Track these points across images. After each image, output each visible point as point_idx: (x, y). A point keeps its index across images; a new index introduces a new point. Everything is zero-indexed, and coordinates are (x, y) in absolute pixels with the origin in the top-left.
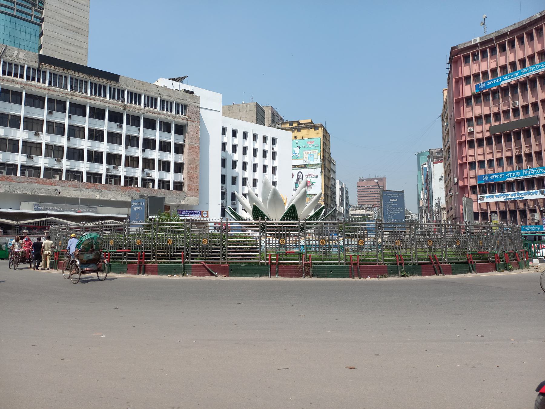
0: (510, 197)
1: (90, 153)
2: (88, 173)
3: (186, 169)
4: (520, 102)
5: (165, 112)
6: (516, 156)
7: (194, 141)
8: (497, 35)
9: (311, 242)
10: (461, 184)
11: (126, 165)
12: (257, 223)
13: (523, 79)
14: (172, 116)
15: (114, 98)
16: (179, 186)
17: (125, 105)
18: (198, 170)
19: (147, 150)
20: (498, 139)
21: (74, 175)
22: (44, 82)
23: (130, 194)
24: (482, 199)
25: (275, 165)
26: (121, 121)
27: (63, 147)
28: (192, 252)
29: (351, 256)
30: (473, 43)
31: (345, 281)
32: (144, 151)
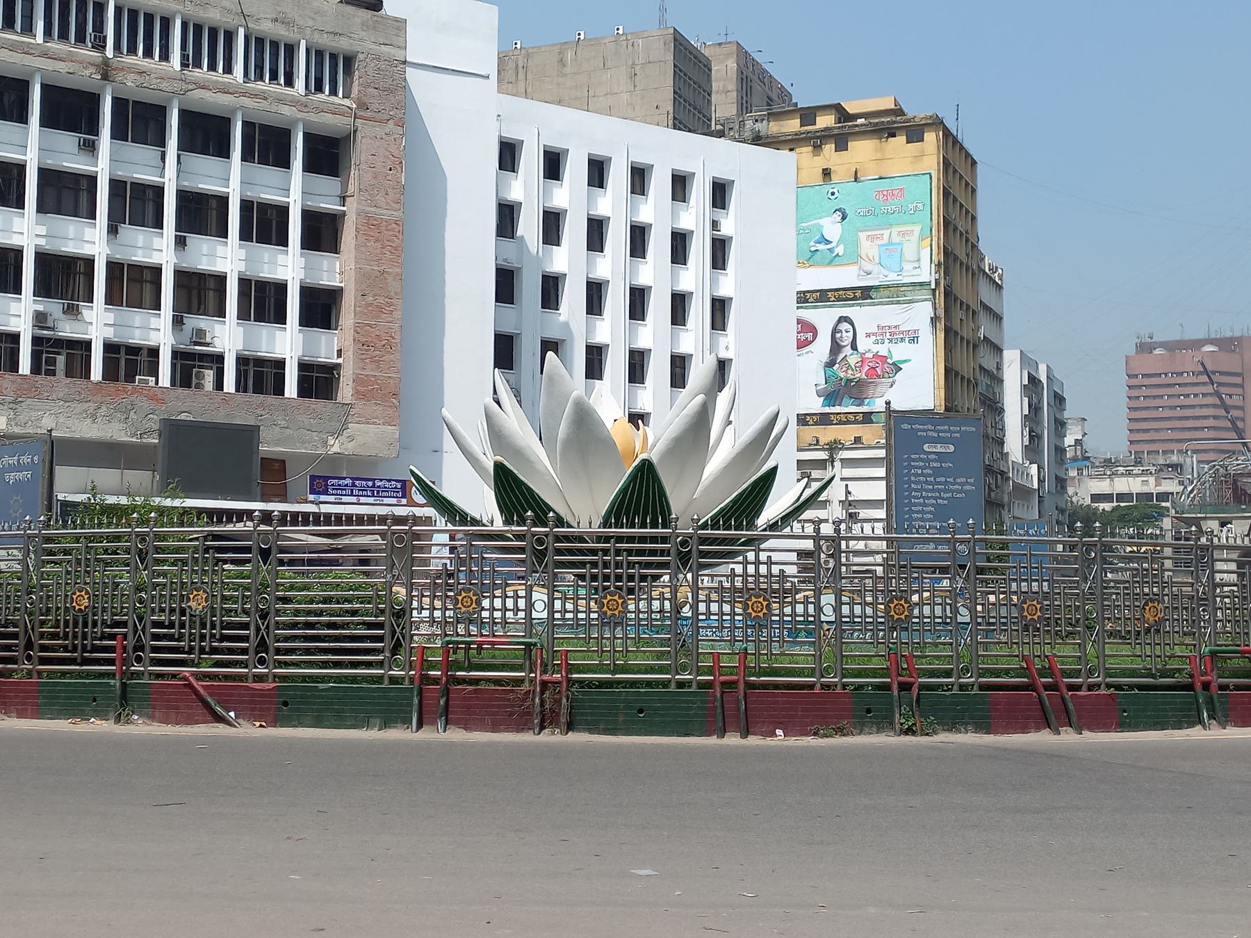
5: (264, 86)
7: (381, 199)
11: (112, 298)
14: (293, 102)
15: (64, 36)
16: (319, 381)
17: (106, 61)
18: (397, 314)
19: (194, 240)
23: (127, 412)
25: (723, 292)
26: (94, 129)
32: (181, 242)
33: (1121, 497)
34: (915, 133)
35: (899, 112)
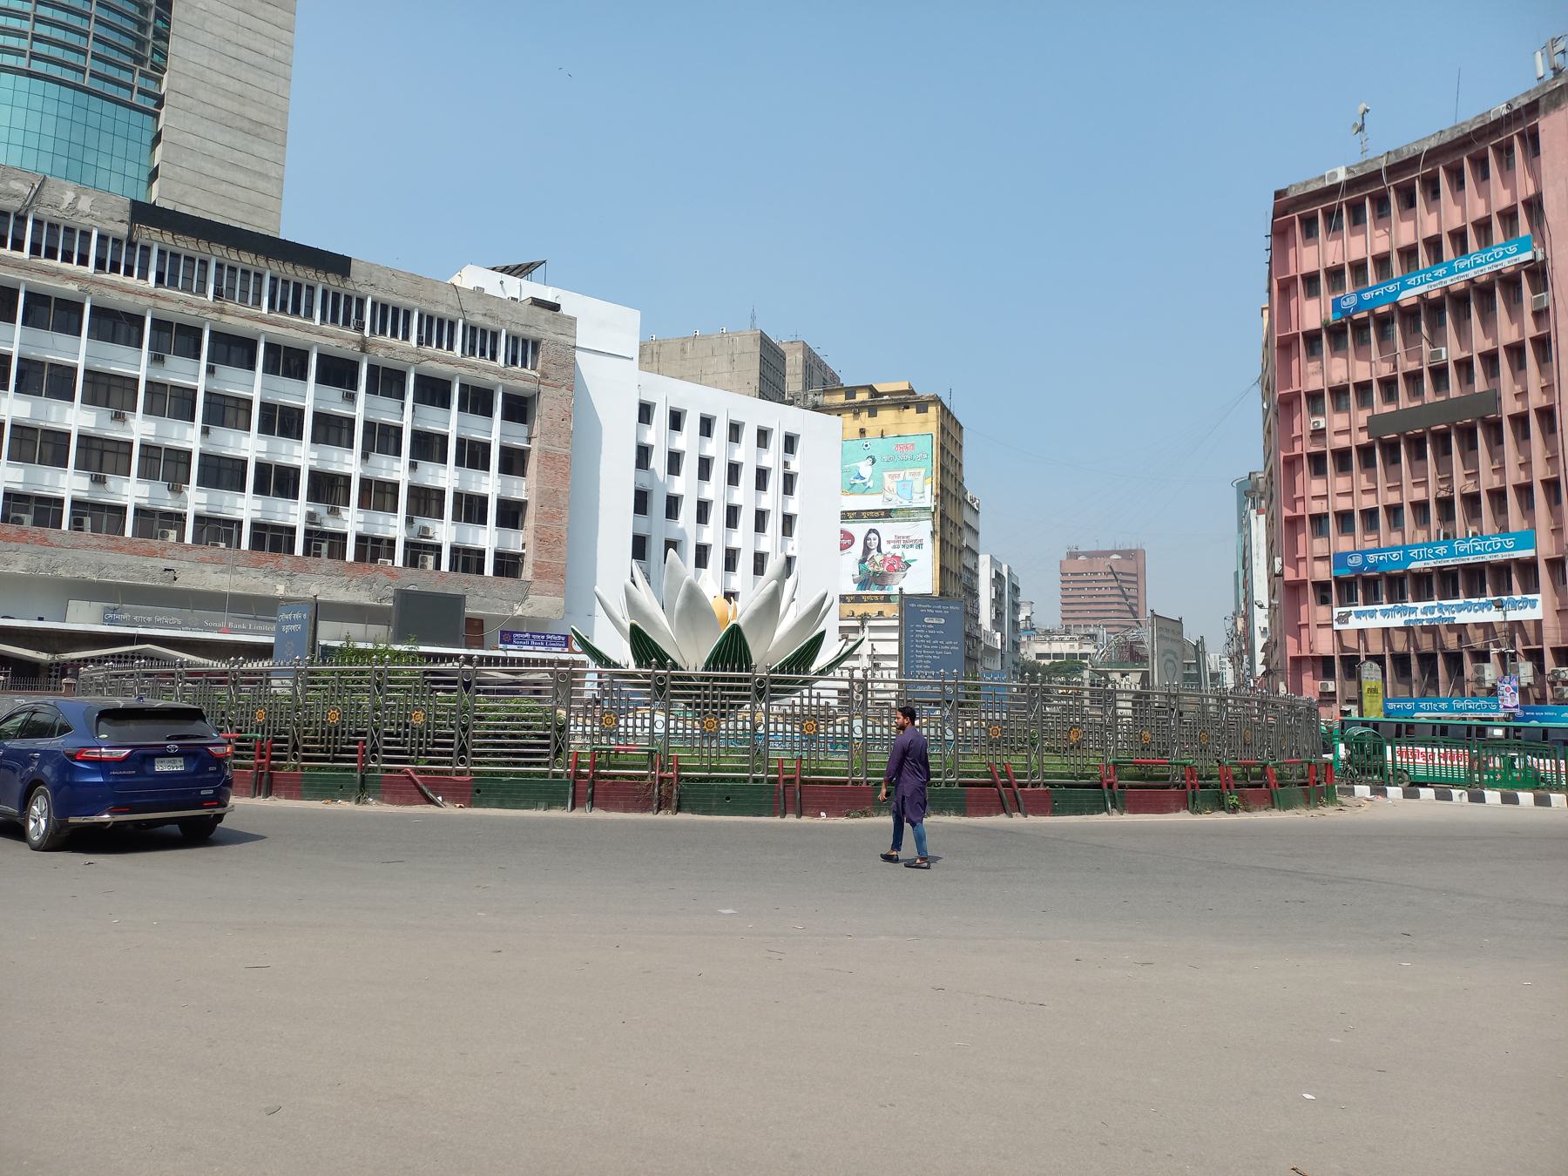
0: (1420, 616)
1: (262, 468)
2: (255, 525)
3: (530, 520)
4: (1451, 351)
5: (476, 360)
6: (1439, 501)
7: (555, 440)
8: (1394, 160)
9: (639, 722)
10: (1290, 575)
11: (363, 504)
12: (647, 676)
13: (1461, 286)
14: (495, 372)
15: (334, 320)
16: (508, 565)
17: (364, 340)
19: (422, 464)
20: (1391, 451)
21: (216, 529)
22: (144, 275)
24: (1343, 619)
26: (354, 385)
27: (189, 454)
28: (387, 743)
29: (781, 762)
30: (1328, 183)
31: (713, 823)
32: (413, 466)
33: (1056, 656)
34: (922, 407)
35: (911, 392)
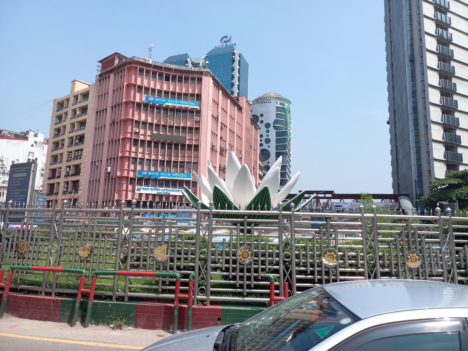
0: (161, 191)
6: (167, 161)
24: (139, 190)
